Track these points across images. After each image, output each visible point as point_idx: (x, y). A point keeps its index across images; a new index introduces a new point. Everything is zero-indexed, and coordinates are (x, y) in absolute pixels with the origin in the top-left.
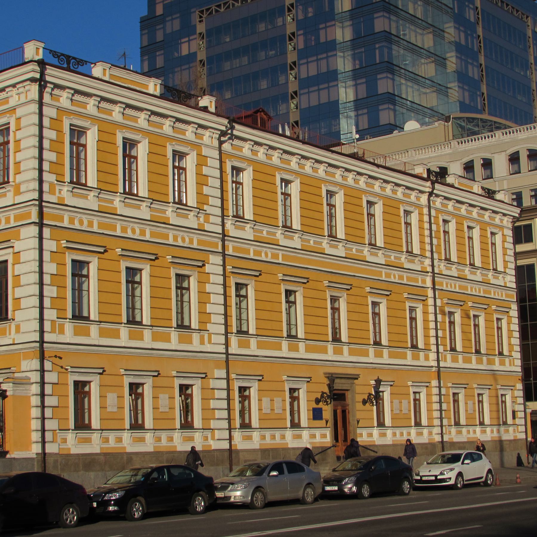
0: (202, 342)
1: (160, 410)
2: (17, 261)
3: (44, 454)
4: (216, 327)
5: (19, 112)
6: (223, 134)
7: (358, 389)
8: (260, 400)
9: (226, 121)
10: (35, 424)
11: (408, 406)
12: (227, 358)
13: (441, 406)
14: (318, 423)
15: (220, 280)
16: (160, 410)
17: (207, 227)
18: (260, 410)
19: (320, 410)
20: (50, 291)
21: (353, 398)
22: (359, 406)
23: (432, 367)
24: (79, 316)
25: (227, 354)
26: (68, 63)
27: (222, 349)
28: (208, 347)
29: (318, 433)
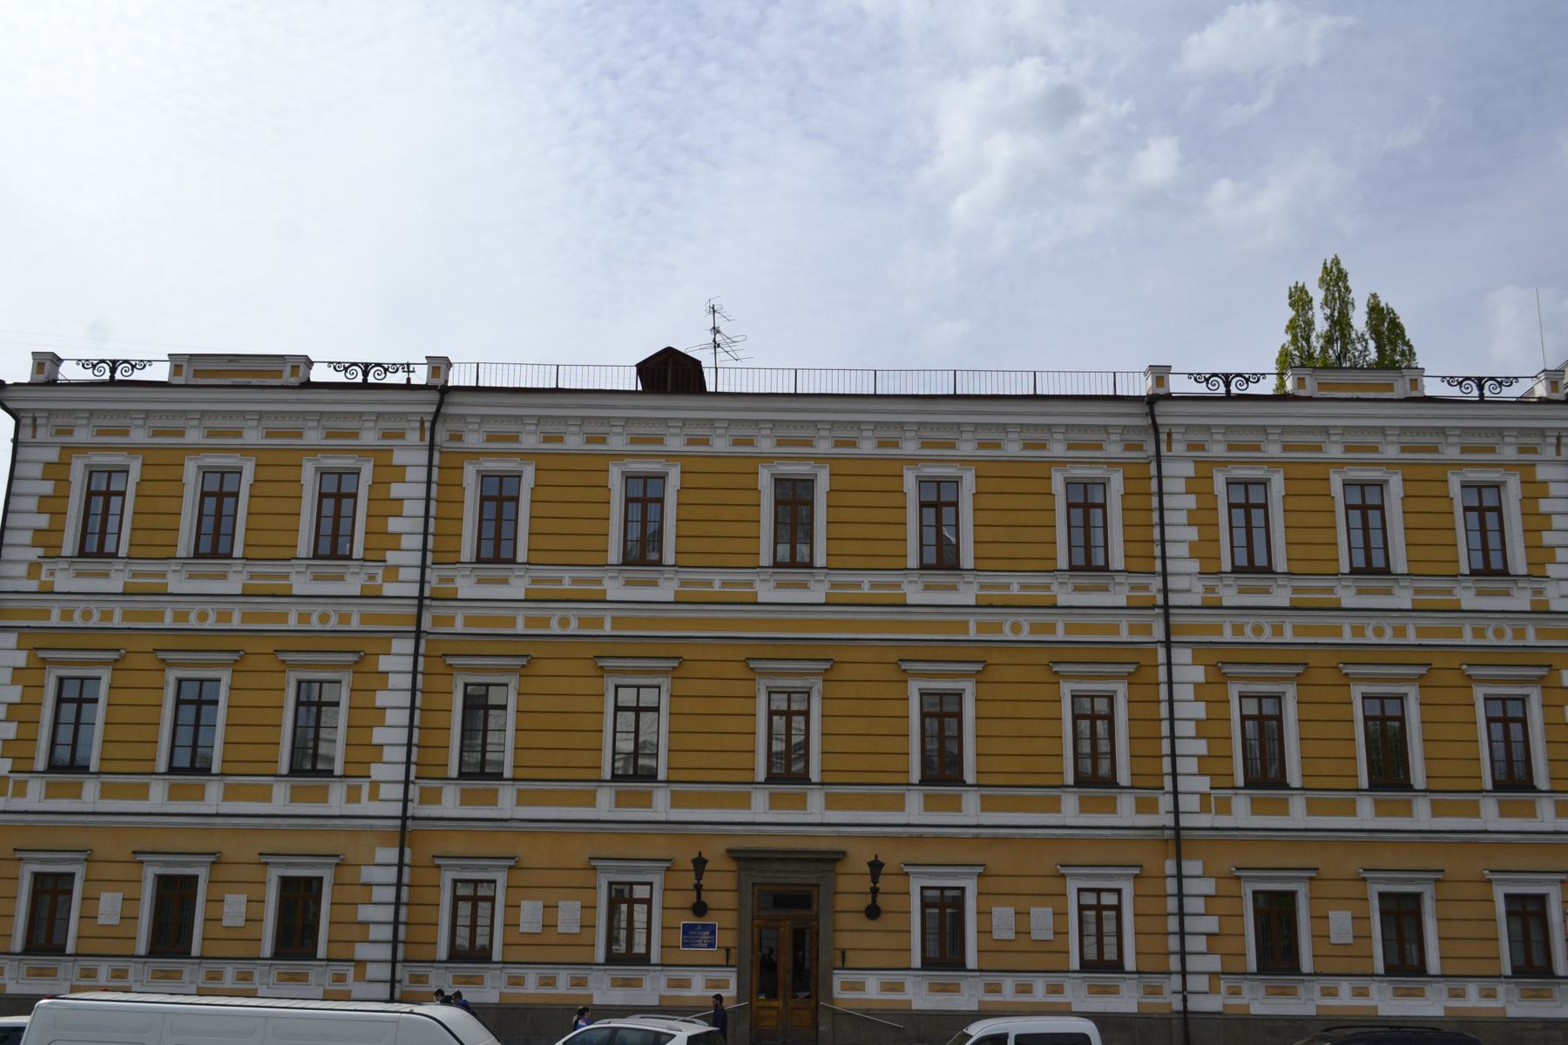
0: (354, 795)
1: (224, 923)
4: (389, 770)
12: (404, 826)
13: (1182, 924)
14: (700, 953)
16: (224, 923)
17: (390, 589)
19: (711, 929)
23: (1163, 828)
28: (366, 807)
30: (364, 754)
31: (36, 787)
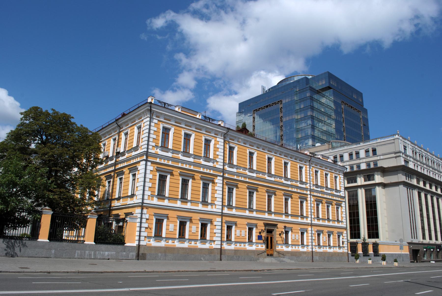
2: (138, 174)
3: (139, 245)
4: (218, 202)
5: (144, 121)
6: (225, 134)
8: (235, 231)
10: (137, 233)
11: (299, 236)
15: (221, 185)
17: (217, 166)
18: (235, 234)
20: (148, 184)
21: (275, 233)
22: (278, 236)
24: (161, 195)
26: (165, 105)
28: (214, 210)
30: (214, 198)
31: (155, 199)
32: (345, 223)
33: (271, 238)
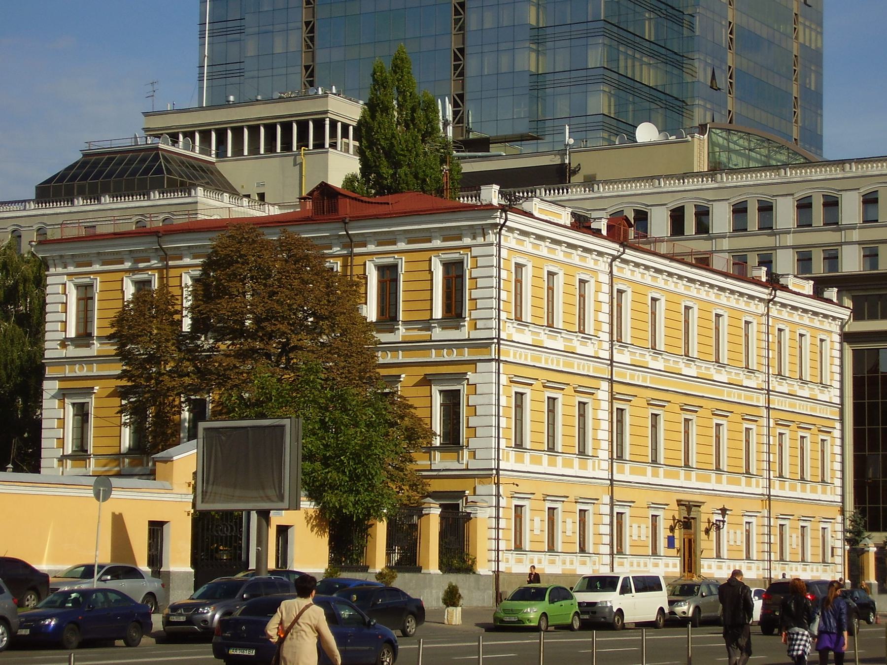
7: (704, 518)
9: (617, 246)
12: (612, 485)
22: (703, 535)
23: (763, 495)
25: (612, 480)
27: (606, 475)
29: (671, 561)
32: (839, 491)
33: (690, 540)
